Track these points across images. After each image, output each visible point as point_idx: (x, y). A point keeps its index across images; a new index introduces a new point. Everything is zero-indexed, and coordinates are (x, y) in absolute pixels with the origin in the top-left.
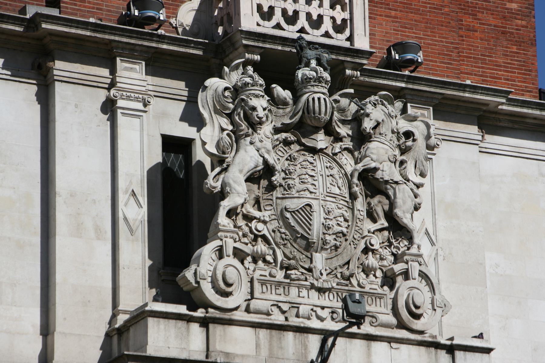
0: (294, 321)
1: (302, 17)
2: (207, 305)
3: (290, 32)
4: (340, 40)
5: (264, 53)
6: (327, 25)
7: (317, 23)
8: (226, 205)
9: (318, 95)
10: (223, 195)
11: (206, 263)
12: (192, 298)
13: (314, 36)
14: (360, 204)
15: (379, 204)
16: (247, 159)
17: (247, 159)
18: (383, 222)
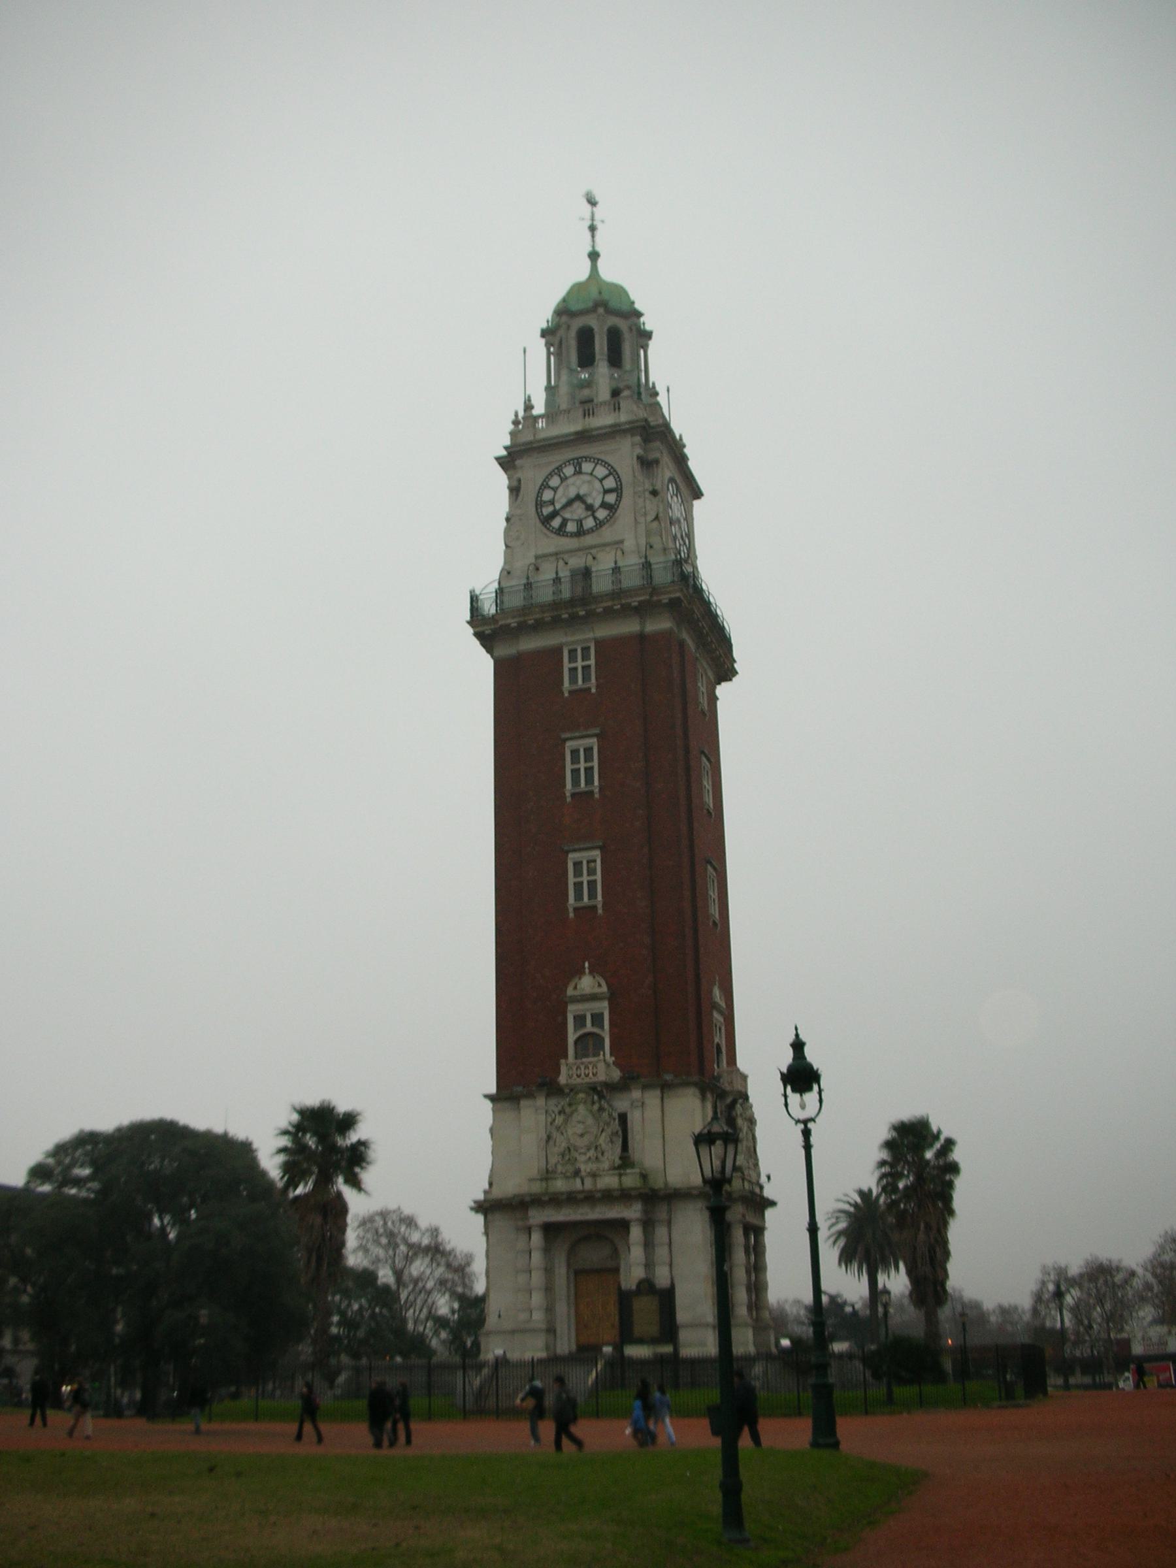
4: (595, 1079)
7: (587, 1076)
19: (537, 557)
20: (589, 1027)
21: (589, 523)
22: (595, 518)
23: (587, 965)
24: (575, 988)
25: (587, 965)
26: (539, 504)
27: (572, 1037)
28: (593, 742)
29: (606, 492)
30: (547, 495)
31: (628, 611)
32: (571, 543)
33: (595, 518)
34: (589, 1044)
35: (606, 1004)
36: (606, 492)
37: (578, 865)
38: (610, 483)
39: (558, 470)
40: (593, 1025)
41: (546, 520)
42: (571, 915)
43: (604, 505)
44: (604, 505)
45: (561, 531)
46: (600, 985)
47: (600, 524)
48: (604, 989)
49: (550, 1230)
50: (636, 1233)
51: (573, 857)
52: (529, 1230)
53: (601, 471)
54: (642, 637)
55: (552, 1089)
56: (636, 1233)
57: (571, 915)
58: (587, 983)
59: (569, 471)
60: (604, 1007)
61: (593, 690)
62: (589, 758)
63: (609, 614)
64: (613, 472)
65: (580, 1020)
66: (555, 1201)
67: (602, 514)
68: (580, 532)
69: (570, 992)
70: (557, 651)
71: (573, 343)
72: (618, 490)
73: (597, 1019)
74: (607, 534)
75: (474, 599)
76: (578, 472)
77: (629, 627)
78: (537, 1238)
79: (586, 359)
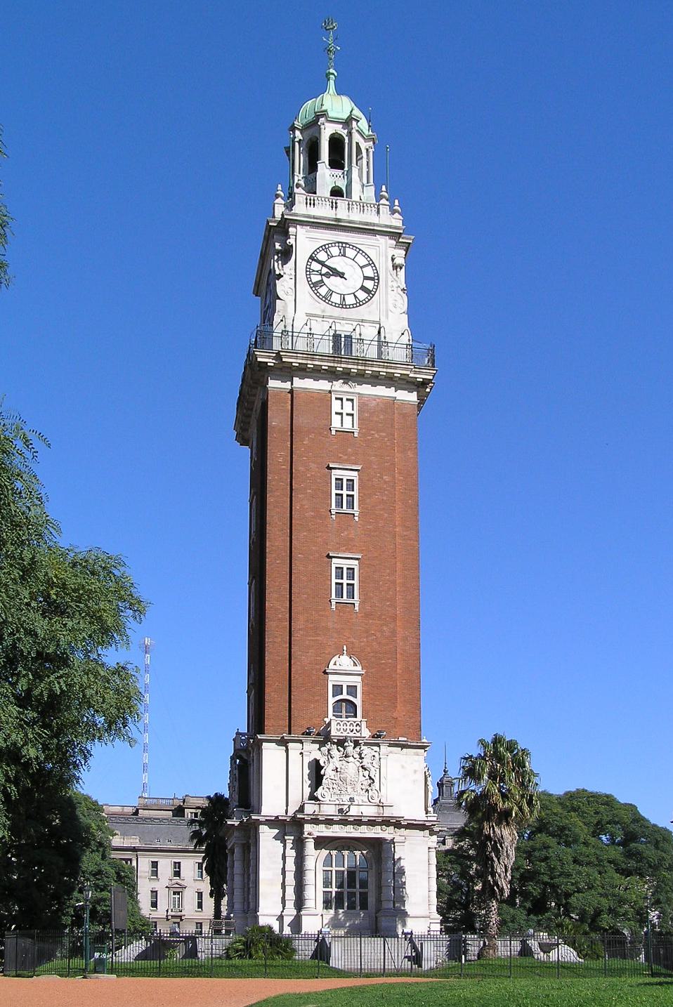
0: (342, 803)
1: (348, 730)
2: (320, 800)
3: (345, 734)
4: (358, 734)
5: (338, 740)
6: (355, 731)
8: (325, 777)
9: (350, 749)
10: (324, 775)
11: (319, 793)
12: (316, 799)
13: (351, 734)
14: (361, 773)
15: (366, 773)
16: (331, 766)
17: (331, 766)
18: (367, 777)
19: (307, 315)
20: (345, 696)
21: (350, 300)
22: (356, 297)
23: (345, 648)
24: (335, 664)
25: (345, 648)
26: (309, 271)
27: (331, 700)
29: (366, 278)
31: (390, 381)
32: (337, 312)
33: (356, 297)
35: (359, 679)
36: (366, 278)
37: (339, 569)
38: (369, 272)
39: (325, 248)
40: (348, 694)
42: (333, 607)
43: (363, 288)
44: (363, 288)
45: (326, 299)
46: (355, 665)
47: (359, 303)
48: (359, 668)
49: (321, 842)
51: (336, 562)
52: (299, 845)
53: (363, 261)
57: (333, 607)
59: (335, 251)
61: (356, 435)
62: (351, 488)
63: (375, 379)
64: (371, 263)
66: (329, 822)
67: (362, 295)
68: (343, 305)
69: (331, 666)
72: (375, 279)
73: (352, 690)
74: (362, 312)
76: (344, 255)
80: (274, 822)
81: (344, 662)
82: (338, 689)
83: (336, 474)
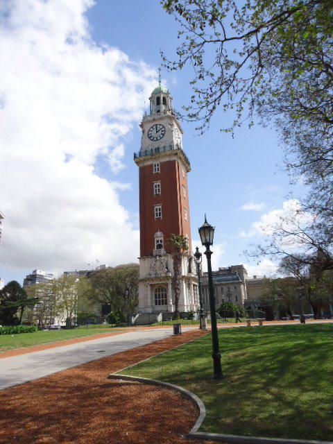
20: (159, 243)
28: (159, 184)
30: (150, 132)
34: (159, 247)
41: (150, 138)
49: (151, 285)
50: (170, 287)
54: (169, 161)
55: (151, 255)
56: (170, 287)
58: (159, 234)
60: (162, 238)
65: (158, 241)
68: (157, 140)
70: (151, 166)
71: (155, 101)
73: (161, 241)
75: (135, 154)
77: (167, 159)
78: (149, 287)
79: (158, 103)
80: (143, 280)
81: (159, 234)
82: (158, 241)
83: (155, 184)
